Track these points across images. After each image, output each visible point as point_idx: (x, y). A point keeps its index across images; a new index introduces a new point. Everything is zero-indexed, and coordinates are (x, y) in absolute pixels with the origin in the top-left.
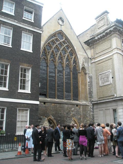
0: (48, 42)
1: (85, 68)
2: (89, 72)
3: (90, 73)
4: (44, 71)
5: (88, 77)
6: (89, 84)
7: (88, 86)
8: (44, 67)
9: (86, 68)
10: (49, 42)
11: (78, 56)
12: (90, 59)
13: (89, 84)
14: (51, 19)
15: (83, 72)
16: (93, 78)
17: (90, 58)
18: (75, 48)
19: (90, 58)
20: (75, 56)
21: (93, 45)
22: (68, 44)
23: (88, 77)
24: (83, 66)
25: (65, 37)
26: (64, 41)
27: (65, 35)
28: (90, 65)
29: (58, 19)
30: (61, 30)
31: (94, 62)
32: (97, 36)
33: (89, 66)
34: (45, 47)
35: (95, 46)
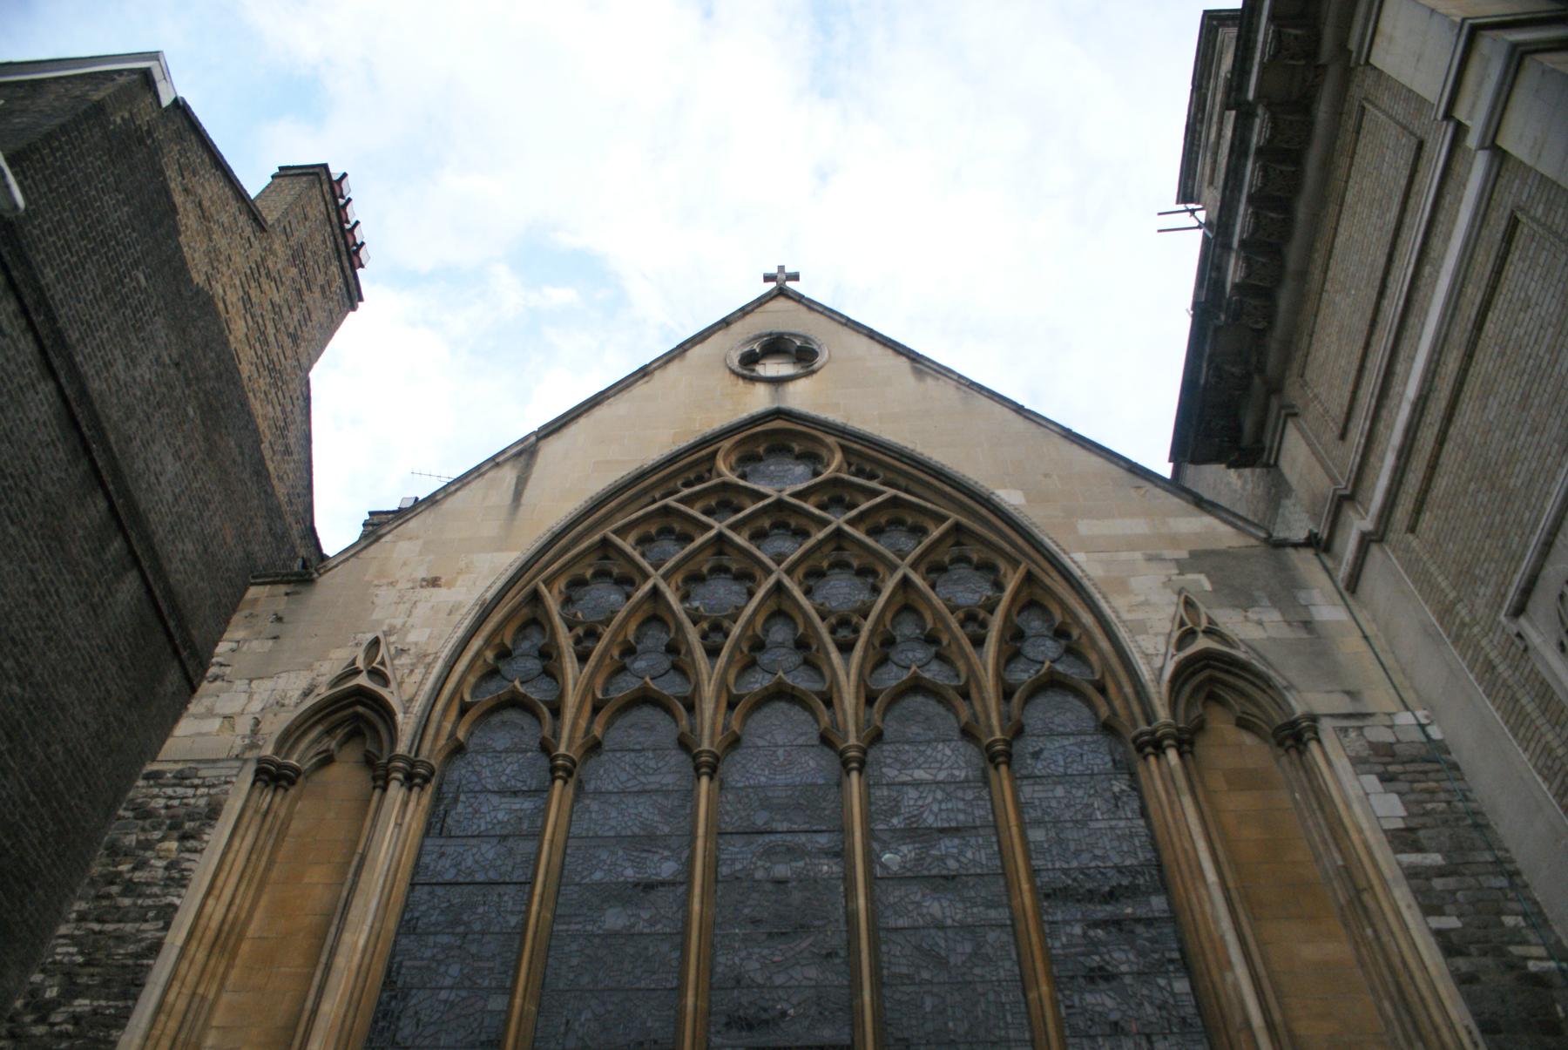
0: (597, 537)
1: (1244, 667)
2: (1348, 693)
3: (1380, 698)
4: (489, 851)
5: (1357, 762)
6: (1412, 874)
7: (1402, 894)
8: (495, 800)
9: (1286, 669)
10: (605, 542)
11: (1081, 562)
12: (1308, 553)
13: (1412, 874)
14: (644, 372)
15: (1248, 739)
16: (1466, 749)
17: (1312, 542)
18: (1010, 498)
19: (1301, 535)
20: (1030, 578)
21: (1275, 388)
22: (894, 502)
23: (1342, 764)
24: (1202, 643)
25: (844, 449)
26: (835, 482)
27: (841, 432)
28: (1328, 611)
29: (750, 360)
30: (778, 413)
31: (1366, 541)
32: (1227, 247)
33: (1307, 625)
34: (535, 598)
35: (1292, 392)
